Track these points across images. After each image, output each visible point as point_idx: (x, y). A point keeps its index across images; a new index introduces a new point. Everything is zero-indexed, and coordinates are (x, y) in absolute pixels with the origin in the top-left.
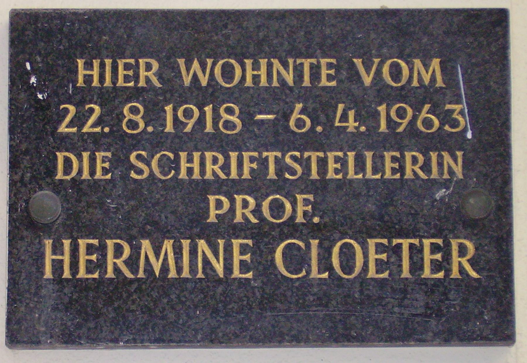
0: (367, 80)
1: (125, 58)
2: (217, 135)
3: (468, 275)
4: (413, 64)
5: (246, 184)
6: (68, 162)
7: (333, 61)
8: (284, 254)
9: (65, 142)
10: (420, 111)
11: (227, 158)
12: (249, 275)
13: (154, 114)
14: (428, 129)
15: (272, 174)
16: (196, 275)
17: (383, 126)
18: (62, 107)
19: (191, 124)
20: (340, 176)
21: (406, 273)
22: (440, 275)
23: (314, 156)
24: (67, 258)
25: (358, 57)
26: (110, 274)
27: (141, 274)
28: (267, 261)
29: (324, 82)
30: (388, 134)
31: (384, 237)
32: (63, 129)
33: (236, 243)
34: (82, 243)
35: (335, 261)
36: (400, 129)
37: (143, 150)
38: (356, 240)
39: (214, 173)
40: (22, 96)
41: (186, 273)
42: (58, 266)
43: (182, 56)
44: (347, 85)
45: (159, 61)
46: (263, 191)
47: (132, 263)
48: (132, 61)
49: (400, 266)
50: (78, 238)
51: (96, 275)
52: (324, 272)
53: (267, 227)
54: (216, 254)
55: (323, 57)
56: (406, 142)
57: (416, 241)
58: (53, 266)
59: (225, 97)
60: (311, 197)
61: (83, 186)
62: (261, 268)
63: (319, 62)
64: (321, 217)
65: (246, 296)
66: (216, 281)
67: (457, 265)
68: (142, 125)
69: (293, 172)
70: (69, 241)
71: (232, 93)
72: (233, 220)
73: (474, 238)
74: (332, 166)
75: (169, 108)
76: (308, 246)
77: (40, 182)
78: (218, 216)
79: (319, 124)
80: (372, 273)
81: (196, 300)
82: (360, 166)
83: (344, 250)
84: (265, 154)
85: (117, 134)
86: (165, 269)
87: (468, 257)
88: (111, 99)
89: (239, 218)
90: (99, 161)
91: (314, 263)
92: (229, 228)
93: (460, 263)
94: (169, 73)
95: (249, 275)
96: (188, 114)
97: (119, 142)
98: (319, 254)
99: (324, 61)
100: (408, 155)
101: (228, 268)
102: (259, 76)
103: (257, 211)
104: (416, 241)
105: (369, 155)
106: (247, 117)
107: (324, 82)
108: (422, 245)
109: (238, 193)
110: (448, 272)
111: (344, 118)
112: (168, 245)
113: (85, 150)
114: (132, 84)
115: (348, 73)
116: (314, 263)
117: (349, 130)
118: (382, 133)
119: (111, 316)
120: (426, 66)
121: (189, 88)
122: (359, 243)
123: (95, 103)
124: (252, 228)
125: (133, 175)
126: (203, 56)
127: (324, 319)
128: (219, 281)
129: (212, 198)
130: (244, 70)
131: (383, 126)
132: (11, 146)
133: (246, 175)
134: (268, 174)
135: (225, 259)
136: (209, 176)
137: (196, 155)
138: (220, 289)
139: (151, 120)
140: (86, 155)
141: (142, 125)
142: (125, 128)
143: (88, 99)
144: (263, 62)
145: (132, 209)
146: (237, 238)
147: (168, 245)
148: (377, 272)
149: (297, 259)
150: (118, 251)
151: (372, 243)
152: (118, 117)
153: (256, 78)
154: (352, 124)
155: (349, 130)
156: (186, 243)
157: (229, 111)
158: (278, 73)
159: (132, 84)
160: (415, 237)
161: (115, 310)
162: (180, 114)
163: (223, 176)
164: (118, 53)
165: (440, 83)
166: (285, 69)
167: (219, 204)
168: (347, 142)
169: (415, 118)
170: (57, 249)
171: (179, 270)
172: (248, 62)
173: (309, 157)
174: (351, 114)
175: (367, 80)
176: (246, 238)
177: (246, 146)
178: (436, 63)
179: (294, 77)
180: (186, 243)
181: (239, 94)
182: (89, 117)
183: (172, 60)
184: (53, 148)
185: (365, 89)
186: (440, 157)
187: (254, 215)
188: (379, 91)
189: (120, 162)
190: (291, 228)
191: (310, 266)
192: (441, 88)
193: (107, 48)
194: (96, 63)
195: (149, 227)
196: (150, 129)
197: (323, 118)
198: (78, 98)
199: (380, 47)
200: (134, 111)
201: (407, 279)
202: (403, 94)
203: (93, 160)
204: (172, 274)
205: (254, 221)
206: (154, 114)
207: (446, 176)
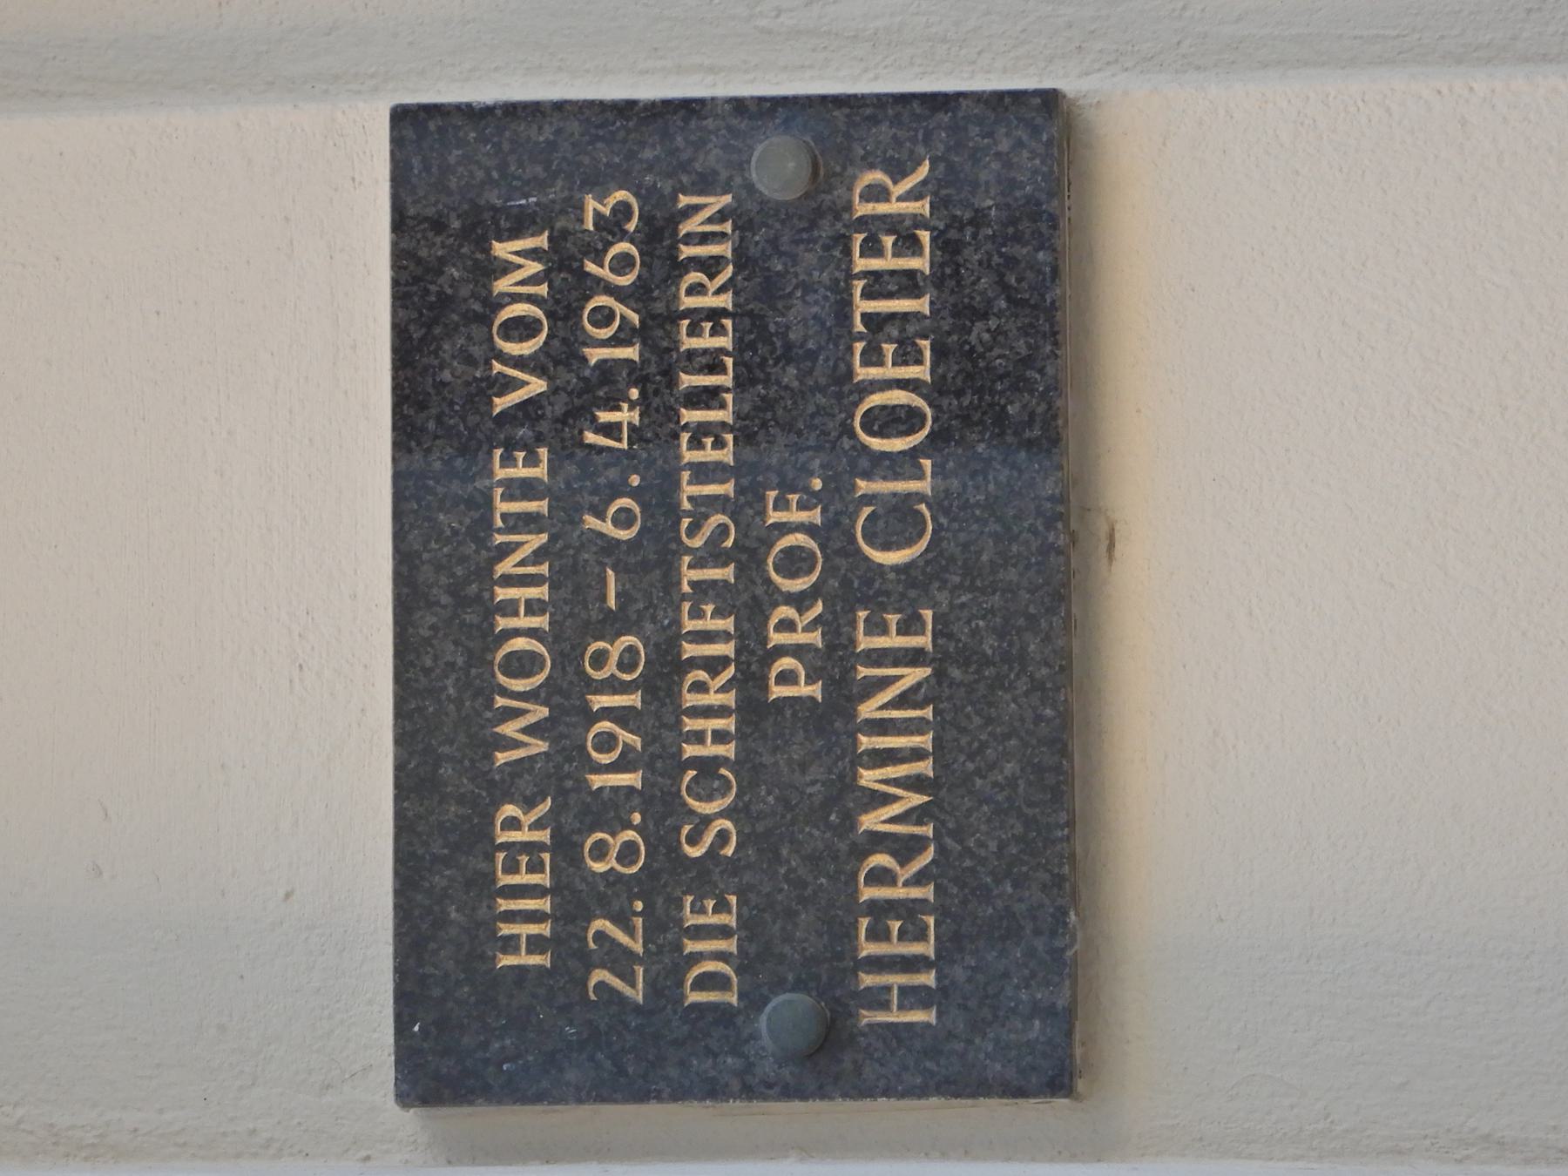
0: (537, 385)
1: (494, 872)
2: (646, 684)
3: (924, 183)
4: (502, 295)
5: (746, 626)
6: (704, 982)
7: (498, 452)
8: (886, 547)
9: (665, 986)
10: (599, 280)
11: (694, 663)
12: (928, 614)
13: (607, 812)
14: (634, 265)
15: (727, 573)
16: (928, 722)
17: (631, 353)
18: (593, 997)
19: (625, 736)
20: (729, 437)
21: (922, 305)
22: (925, 236)
23: (689, 490)
24: (896, 980)
25: (490, 404)
26: (927, 892)
27: (928, 830)
28: (899, 581)
29: (540, 472)
30: (644, 343)
31: (850, 349)
32: (637, 994)
33: (865, 643)
34: (868, 949)
35: (898, 444)
36: (635, 318)
37: (678, 830)
38: (856, 404)
39: (723, 689)
40: (571, 1075)
41: (924, 741)
42: (912, 996)
43: (489, 758)
44: (544, 427)
45: (496, 805)
46: (759, 590)
47: (905, 849)
48: (501, 856)
49: (905, 316)
50: (854, 958)
51: (931, 921)
52: (920, 467)
53: (831, 582)
54: (886, 682)
55: (491, 474)
56: (659, 307)
57: (859, 285)
58: (911, 1009)
59: (570, 669)
60: (772, 495)
61: (752, 949)
62: (912, 593)
63: (501, 483)
64: (811, 474)
65: (969, 622)
66: (939, 683)
67: (904, 205)
68: (630, 835)
69: (723, 530)
70: (862, 975)
71: (562, 654)
72: (817, 650)
73: (850, 171)
74: (709, 455)
75: (597, 781)
76: (868, 499)
77: (745, 1034)
78: (810, 680)
79: (625, 482)
80: (921, 372)
81: (977, 721)
82: (709, 397)
83: (876, 428)
84: (686, 588)
85: (647, 884)
86: (914, 783)
87: (889, 182)
88: (575, 900)
89: (816, 638)
90: (701, 920)
91: (901, 486)
92: (834, 661)
93: (900, 199)
94: (520, 783)
95: (928, 614)
96: (606, 742)
97: (666, 877)
98: (885, 478)
99: (501, 473)
100: (689, 302)
101: (914, 657)
102: (528, 602)
103: (799, 601)
104: (859, 285)
105: (688, 380)
106: (612, 625)
107: (540, 472)
108: (866, 274)
109: (765, 640)
110: (918, 222)
111: (611, 430)
112: (869, 777)
113: (679, 947)
114: (546, 857)
115: (523, 425)
116: (901, 486)
117: (636, 421)
118: (641, 355)
119: (1009, 889)
120: (507, 268)
121: (554, 741)
122: (861, 400)
123: (586, 929)
124: (834, 613)
125: (729, 851)
126: (489, 715)
127: (1013, 466)
128: (939, 674)
129: (778, 691)
130: (517, 633)
131: (631, 353)
132: (675, 1098)
133: (728, 624)
134: (725, 581)
135: (895, 665)
136: (730, 699)
137: (691, 724)
138: (956, 673)
139: (620, 819)
140: (691, 946)
141: (630, 835)
142: (634, 869)
143: (576, 945)
144: (503, 594)
145: (797, 852)
146: (853, 642)
147: (869, 777)
148: (919, 362)
149: (897, 520)
150: (881, 877)
151: (863, 373)
152: (614, 884)
153: (533, 607)
154: (625, 416)
155: (636, 421)
156: (866, 742)
157: (600, 659)
158: (522, 563)
159: (546, 857)
160: (849, 290)
161: (998, 882)
162: (605, 759)
163: (730, 671)
164: (484, 886)
165: (542, 241)
166: (513, 551)
167: (786, 678)
168: (661, 426)
169: (611, 290)
170: (878, 998)
171: (917, 754)
172: (503, 623)
173: (690, 499)
174: (605, 417)
175: (537, 385)
176: (853, 623)
177: (670, 625)
178: (502, 250)
179: (530, 532)
180: (866, 742)
181: (567, 641)
182: (613, 941)
183: (497, 777)
184: (675, 1012)
185: (554, 391)
186: (689, 239)
187: (808, 609)
188: (557, 363)
189: (705, 877)
190: (833, 533)
191: (909, 496)
192: (550, 239)
193: (474, 909)
194: (506, 929)
195: (833, 817)
196: (637, 818)
197: (613, 473)
198: (572, 963)
199: (470, 361)
200: (600, 851)
201: (932, 303)
202: (564, 311)
203: (699, 932)
204: (925, 767)
205: (819, 608)
206: (607, 812)
207: (728, 227)
